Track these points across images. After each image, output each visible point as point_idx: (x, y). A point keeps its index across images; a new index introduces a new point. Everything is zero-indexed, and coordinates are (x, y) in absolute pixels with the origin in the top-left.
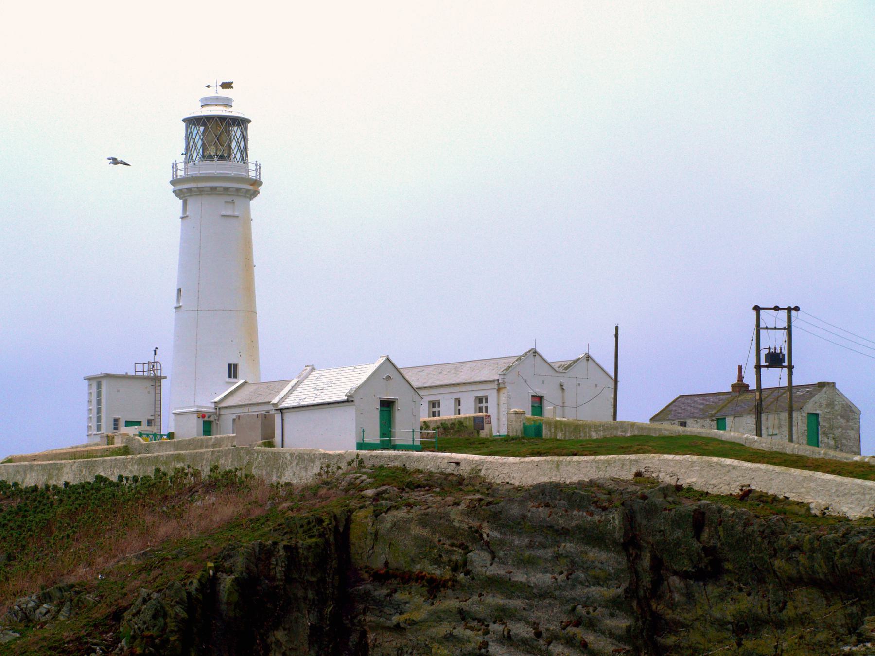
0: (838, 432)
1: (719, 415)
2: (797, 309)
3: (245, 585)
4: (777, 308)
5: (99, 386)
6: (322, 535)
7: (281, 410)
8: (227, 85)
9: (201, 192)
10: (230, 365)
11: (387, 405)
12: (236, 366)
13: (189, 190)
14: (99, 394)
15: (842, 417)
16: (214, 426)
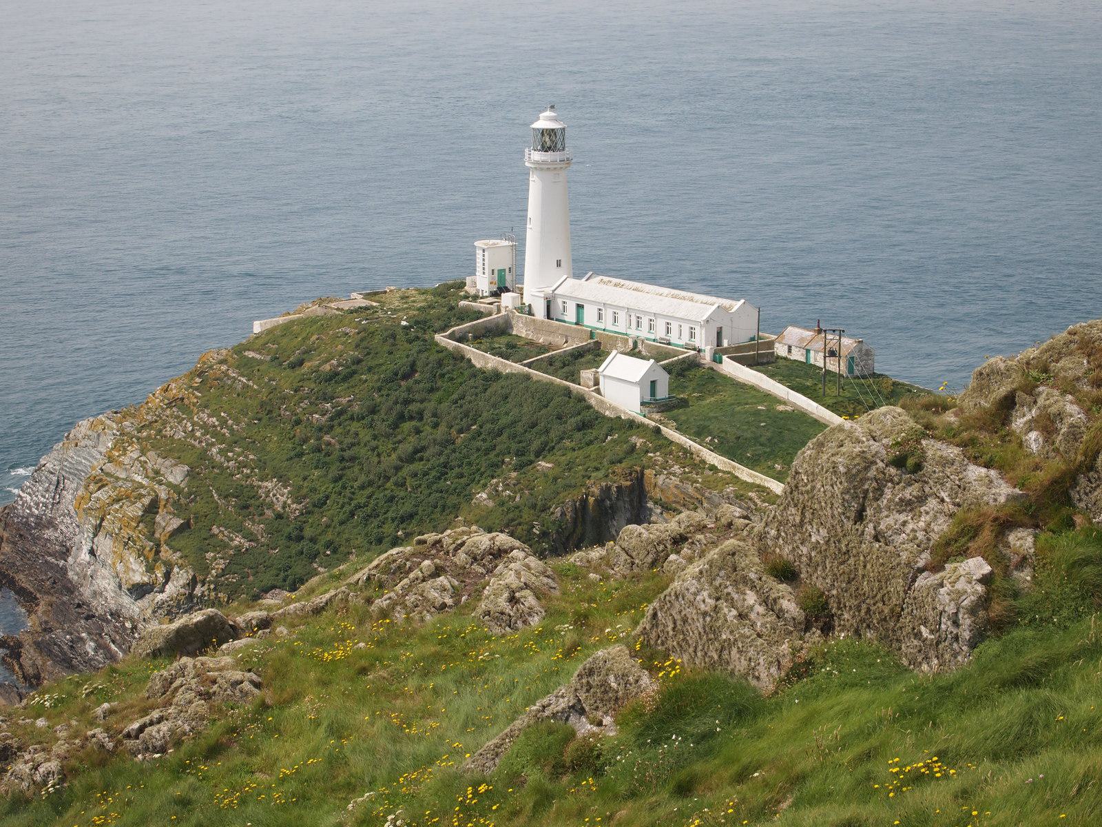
1: (807, 347)
2: (843, 331)
3: (599, 502)
6: (631, 480)
7: (604, 376)
8: (552, 107)
11: (653, 383)
15: (865, 355)
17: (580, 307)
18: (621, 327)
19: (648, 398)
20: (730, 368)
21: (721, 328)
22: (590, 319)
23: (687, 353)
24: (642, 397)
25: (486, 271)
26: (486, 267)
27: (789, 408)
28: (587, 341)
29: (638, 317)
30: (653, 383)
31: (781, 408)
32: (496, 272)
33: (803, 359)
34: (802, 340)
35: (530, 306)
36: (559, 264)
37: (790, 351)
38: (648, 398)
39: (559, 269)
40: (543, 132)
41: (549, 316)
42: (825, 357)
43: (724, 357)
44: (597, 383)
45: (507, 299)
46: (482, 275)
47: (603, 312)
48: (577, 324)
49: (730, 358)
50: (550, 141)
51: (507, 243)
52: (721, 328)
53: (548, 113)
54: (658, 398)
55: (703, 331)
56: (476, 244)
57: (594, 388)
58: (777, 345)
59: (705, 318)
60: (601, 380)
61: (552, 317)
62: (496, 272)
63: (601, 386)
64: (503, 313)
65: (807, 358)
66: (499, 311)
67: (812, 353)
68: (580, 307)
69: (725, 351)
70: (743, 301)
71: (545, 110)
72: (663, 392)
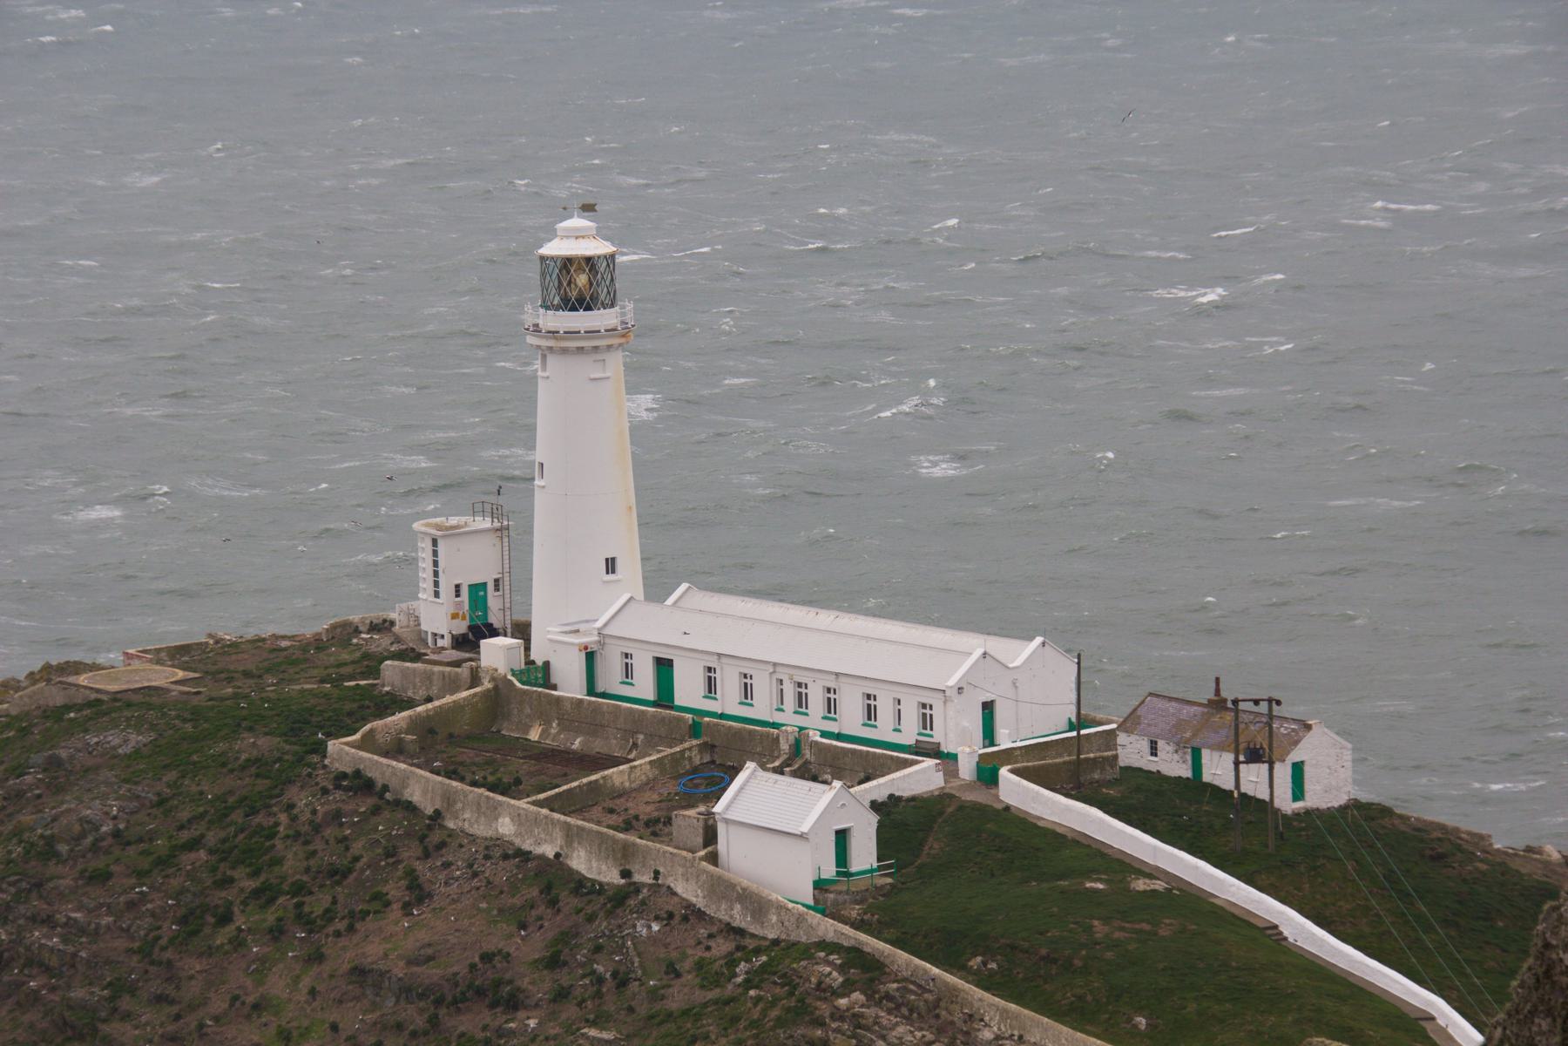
2: (1278, 703)
4: (1256, 702)
5: (435, 543)
7: (727, 821)
8: (588, 208)
9: (564, 351)
11: (842, 836)
12: (613, 559)
13: (550, 348)
14: (435, 553)
16: (598, 659)
17: (664, 666)
18: (762, 708)
19: (830, 871)
22: (689, 692)
23: (917, 762)
25: (442, 589)
26: (442, 579)
27: (1159, 885)
28: (682, 741)
29: (800, 685)
30: (842, 836)
31: (1141, 885)
32: (465, 592)
34: (1180, 725)
35: (547, 664)
36: (611, 565)
37: (1154, 752)
38: (830, 871)
40: (567, 263)
41: (591, 690)
42: (1237, 763)
43: (1004, 772)
44: (710, 836)
45: (497, 653)
46: (432, 599)
48: (655, 704)
49: (1012, 771)
51: (486, 523)
53: (577, 222)
54: (853, 869)
57: (702, 853)
58: (1122, 738)
59: (952, 682)
62: (465, 592)
63: (722, 846)
64: (488, 684)
66: (475, 679)
67: (1206, 754)
68: (664, 666)
69: (1007, 756)
70: (1039, 640)
71: (566, 213)
72: (864, 855)
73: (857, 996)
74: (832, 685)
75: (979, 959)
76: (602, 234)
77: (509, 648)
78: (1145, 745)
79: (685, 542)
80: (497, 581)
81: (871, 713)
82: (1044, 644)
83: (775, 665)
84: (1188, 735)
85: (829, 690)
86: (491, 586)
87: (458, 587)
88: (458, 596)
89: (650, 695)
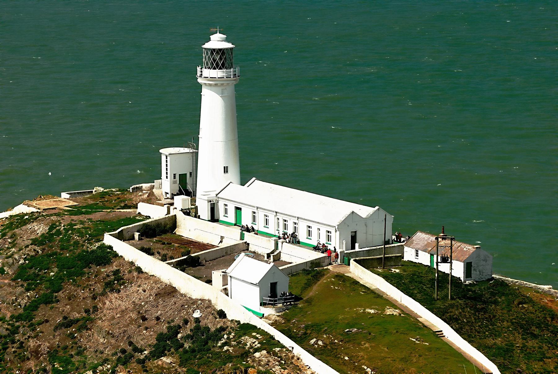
0: (481, 268)
10: (224, 167)
11: (273, 286)
12: (227, 167)
15: (483, 260)
20: (356, 271)
21: (355, 232)
24: (261, 298)
25: (169, 176)
27: (396, 312)
30: (273, 286)
33: (429, 264)
34: (428, 245)
36: (226, 170)
39: (226, 175)
43: (352, 261)
47: (256, 215)
50: (221, 59)
52: (355, 232)
55: (338, 232)
56: (161, 151)
58: (406, 249)
60: (229, 278)
61: (216, 218)
65: (432, 261)
68: (238, 209)
73: (264, 352)
74: (296, 221)
75: (315, 340)
76: (227, 40)
77: (183, 200)
78: (414, 251)
79: (253, 162)
80: (191, 173)
81: (309, 233)
82: (378, 209)
83: (276, 212)
84: (430, 249)
85: (295, 223)
86: (188, 175)
87: (175, 175)
88: (175, 178)
89: (233, 222)
